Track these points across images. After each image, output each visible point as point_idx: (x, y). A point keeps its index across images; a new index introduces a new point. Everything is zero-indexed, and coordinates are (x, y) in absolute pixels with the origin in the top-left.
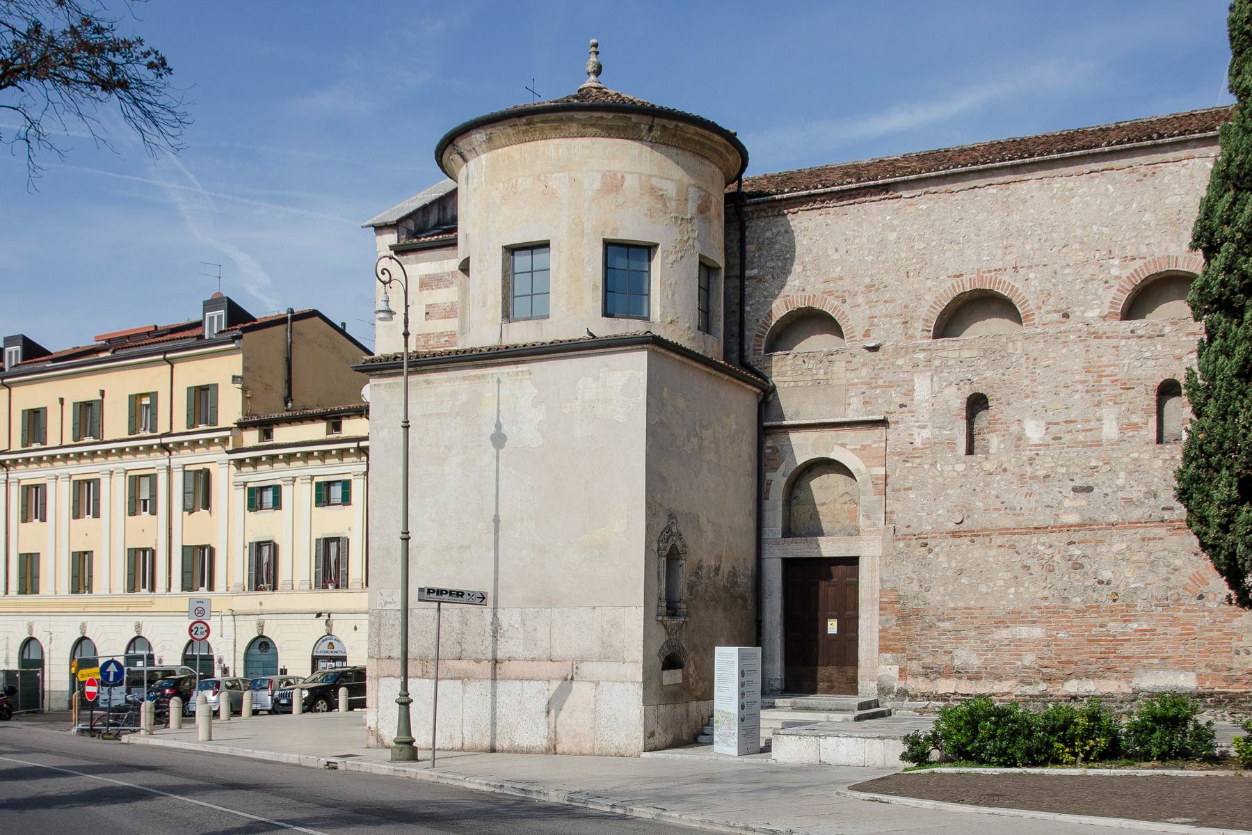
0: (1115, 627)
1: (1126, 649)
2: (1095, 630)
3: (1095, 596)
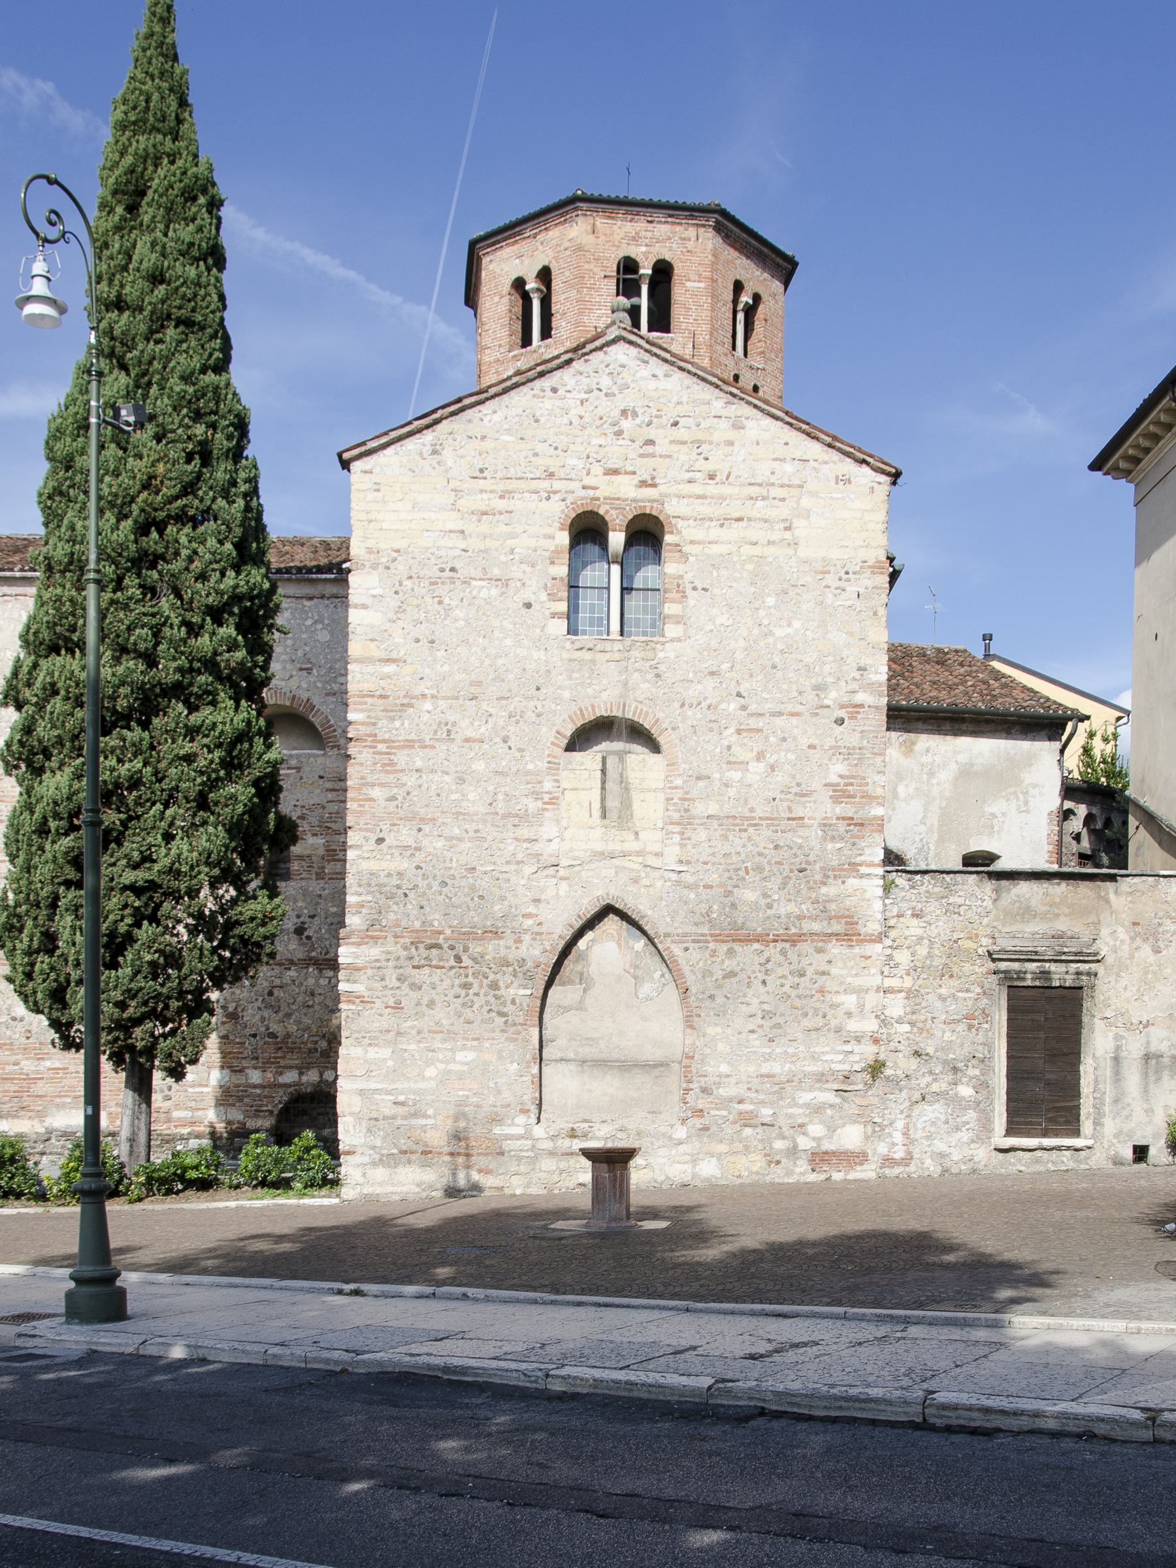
0: (28, 1065)
1: (41, 1088)
2: (8, 1068)
3: (9, 1033)
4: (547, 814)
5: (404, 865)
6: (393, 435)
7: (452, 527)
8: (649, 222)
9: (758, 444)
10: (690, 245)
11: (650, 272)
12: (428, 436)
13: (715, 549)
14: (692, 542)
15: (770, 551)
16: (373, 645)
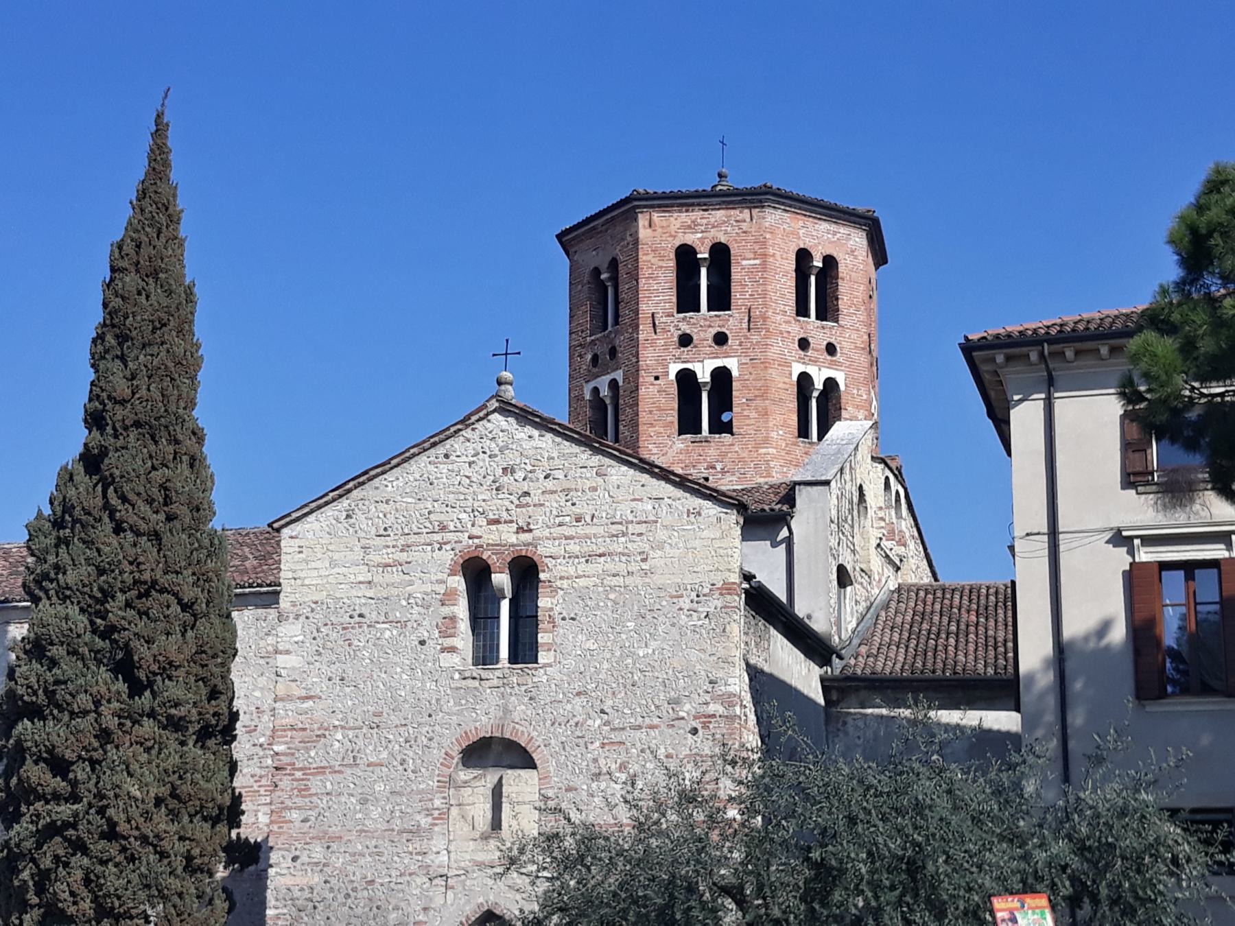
4: (436, 829)
5: (316, 879)
6: (313, 505)
7: (362, 579)
9: (618, 487)
10: (745, 226)
11: (706, 256)
12: (345, 503)
13: (582, 582)
14: (561, 578)
15: (629, 580)
16: (293, 684)
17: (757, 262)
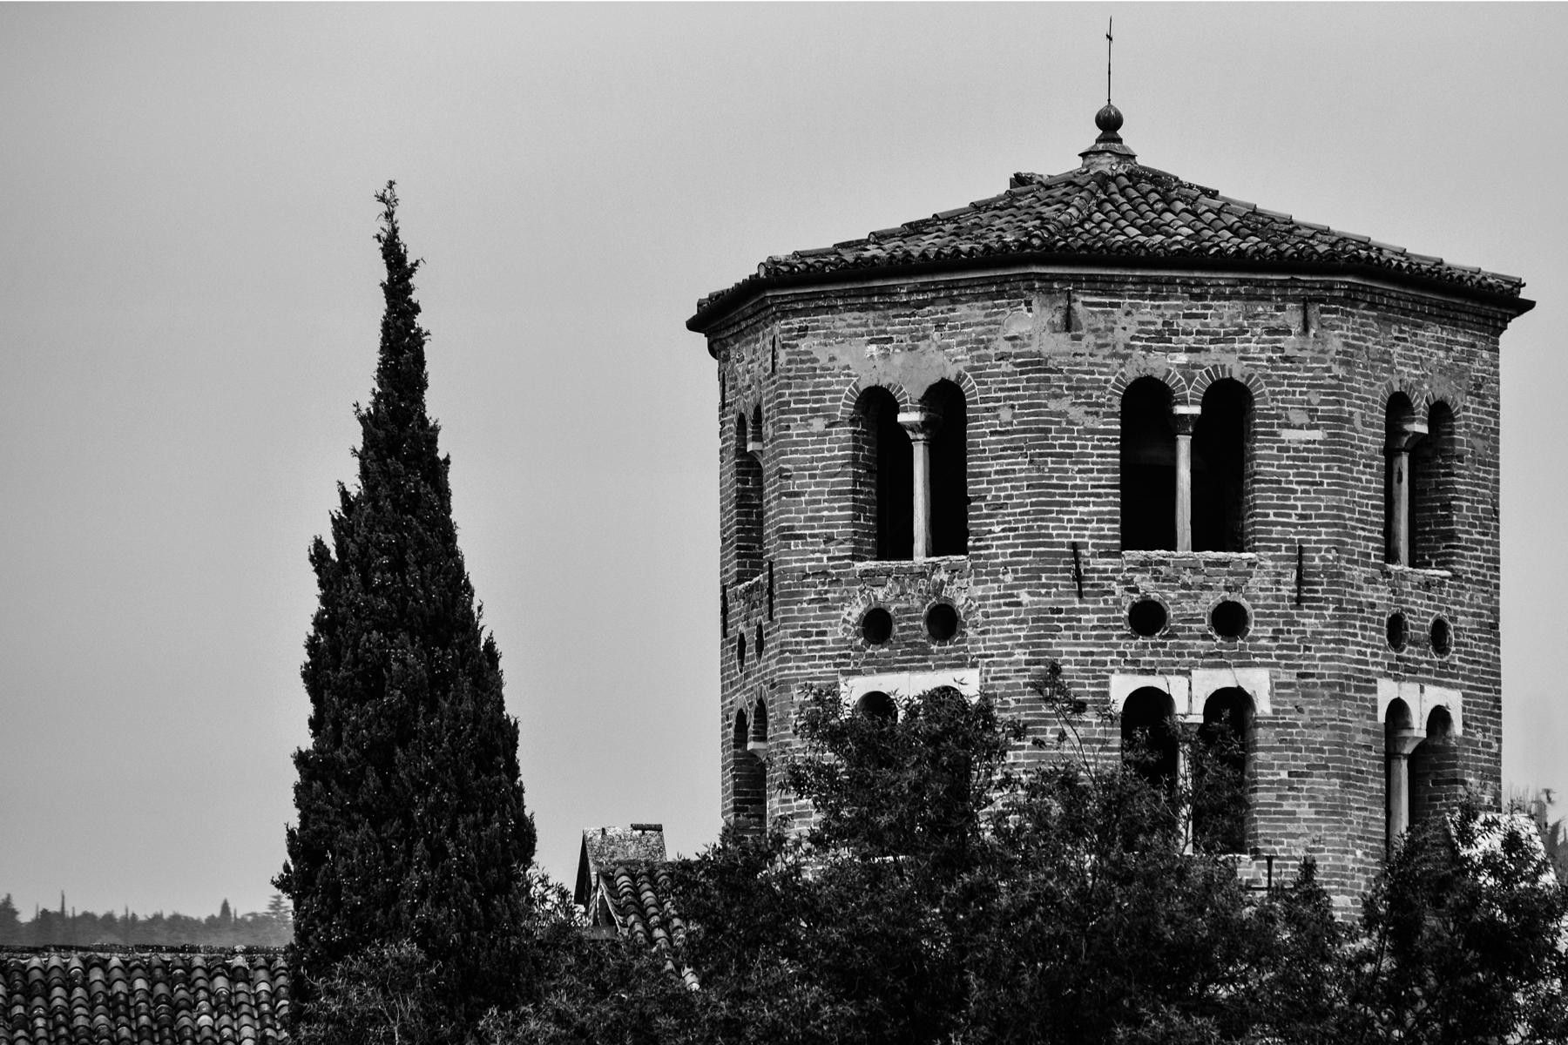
8: (1193, 297)
10: (1290, 343)
17: (1318, 435)
